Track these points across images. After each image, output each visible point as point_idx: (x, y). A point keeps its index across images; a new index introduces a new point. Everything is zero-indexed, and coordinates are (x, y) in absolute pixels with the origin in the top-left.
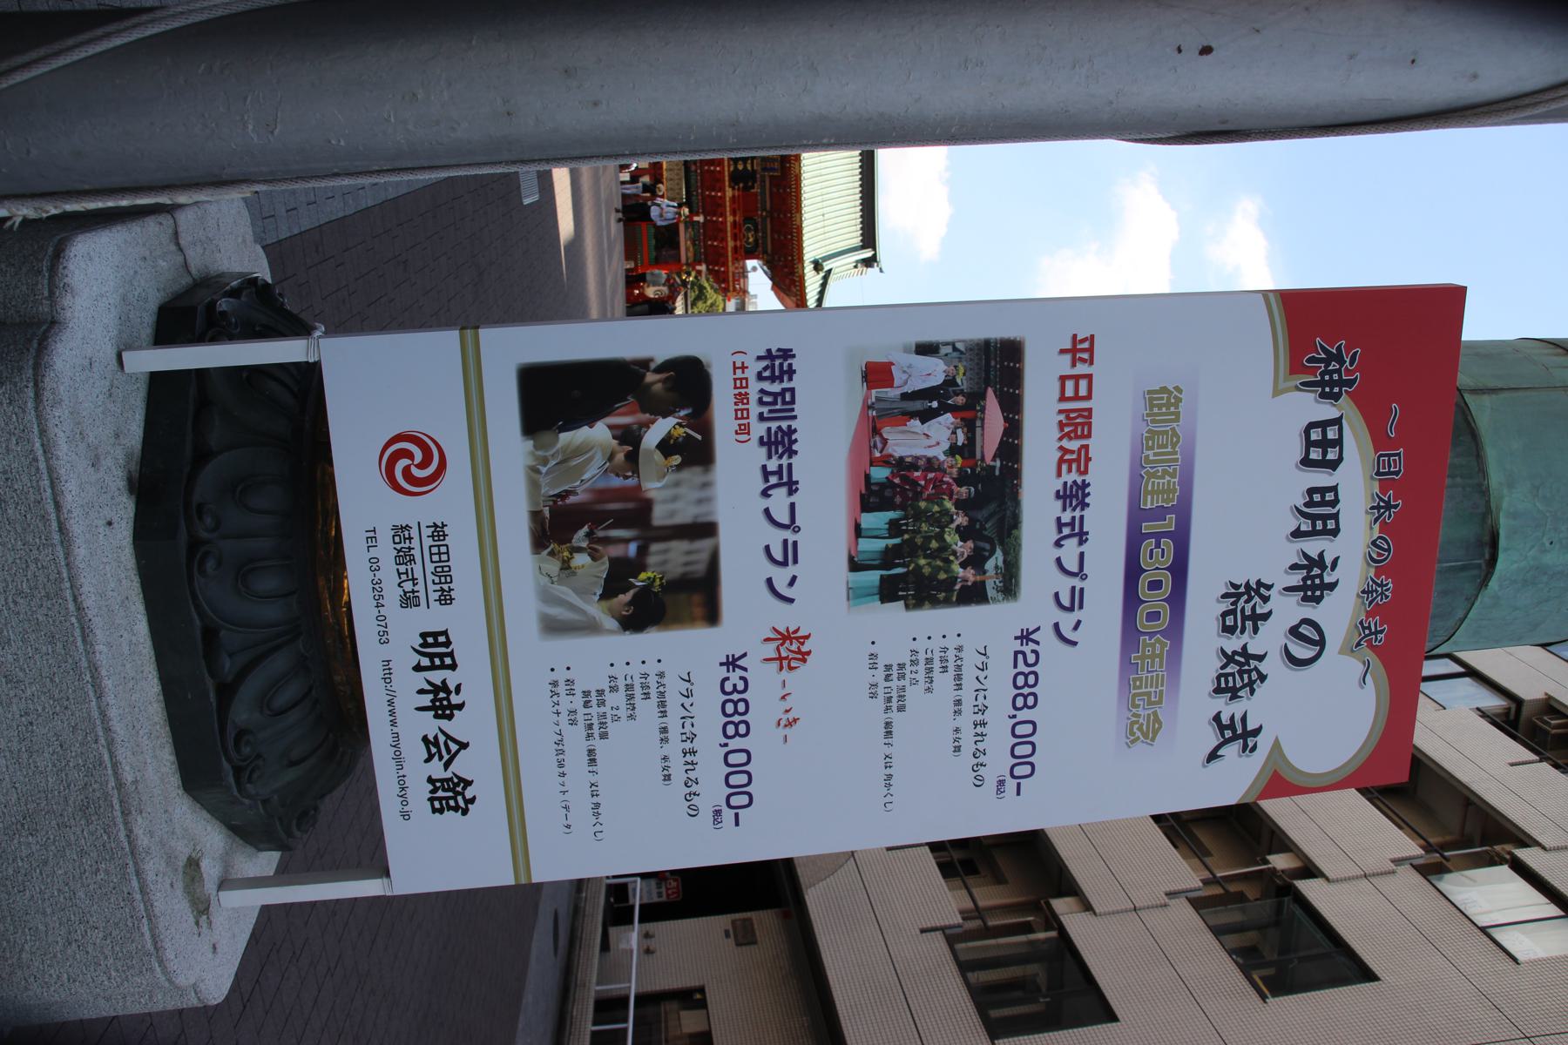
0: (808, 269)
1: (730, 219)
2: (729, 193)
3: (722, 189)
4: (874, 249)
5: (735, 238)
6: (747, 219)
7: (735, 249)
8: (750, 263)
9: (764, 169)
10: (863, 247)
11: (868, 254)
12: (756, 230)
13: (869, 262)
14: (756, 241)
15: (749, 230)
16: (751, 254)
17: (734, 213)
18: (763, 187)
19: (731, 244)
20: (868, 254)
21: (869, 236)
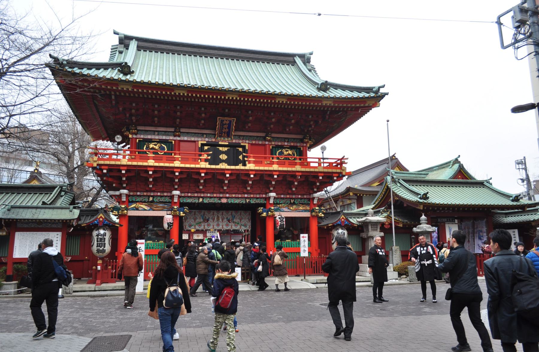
2: (250, 166)
3: (247, 173)
4: (293, 55)
7: (302, 164)
9: (228, 135)
10: (294, 63)
11: (298, 60)
12: (282, 147)
13: (306, 59)
14: (291, 148)
15: (281, 153)
16: (302, 154)
17: (272, 163)
18: (244, 138)
20: (298, 60)
21: (285, 59)
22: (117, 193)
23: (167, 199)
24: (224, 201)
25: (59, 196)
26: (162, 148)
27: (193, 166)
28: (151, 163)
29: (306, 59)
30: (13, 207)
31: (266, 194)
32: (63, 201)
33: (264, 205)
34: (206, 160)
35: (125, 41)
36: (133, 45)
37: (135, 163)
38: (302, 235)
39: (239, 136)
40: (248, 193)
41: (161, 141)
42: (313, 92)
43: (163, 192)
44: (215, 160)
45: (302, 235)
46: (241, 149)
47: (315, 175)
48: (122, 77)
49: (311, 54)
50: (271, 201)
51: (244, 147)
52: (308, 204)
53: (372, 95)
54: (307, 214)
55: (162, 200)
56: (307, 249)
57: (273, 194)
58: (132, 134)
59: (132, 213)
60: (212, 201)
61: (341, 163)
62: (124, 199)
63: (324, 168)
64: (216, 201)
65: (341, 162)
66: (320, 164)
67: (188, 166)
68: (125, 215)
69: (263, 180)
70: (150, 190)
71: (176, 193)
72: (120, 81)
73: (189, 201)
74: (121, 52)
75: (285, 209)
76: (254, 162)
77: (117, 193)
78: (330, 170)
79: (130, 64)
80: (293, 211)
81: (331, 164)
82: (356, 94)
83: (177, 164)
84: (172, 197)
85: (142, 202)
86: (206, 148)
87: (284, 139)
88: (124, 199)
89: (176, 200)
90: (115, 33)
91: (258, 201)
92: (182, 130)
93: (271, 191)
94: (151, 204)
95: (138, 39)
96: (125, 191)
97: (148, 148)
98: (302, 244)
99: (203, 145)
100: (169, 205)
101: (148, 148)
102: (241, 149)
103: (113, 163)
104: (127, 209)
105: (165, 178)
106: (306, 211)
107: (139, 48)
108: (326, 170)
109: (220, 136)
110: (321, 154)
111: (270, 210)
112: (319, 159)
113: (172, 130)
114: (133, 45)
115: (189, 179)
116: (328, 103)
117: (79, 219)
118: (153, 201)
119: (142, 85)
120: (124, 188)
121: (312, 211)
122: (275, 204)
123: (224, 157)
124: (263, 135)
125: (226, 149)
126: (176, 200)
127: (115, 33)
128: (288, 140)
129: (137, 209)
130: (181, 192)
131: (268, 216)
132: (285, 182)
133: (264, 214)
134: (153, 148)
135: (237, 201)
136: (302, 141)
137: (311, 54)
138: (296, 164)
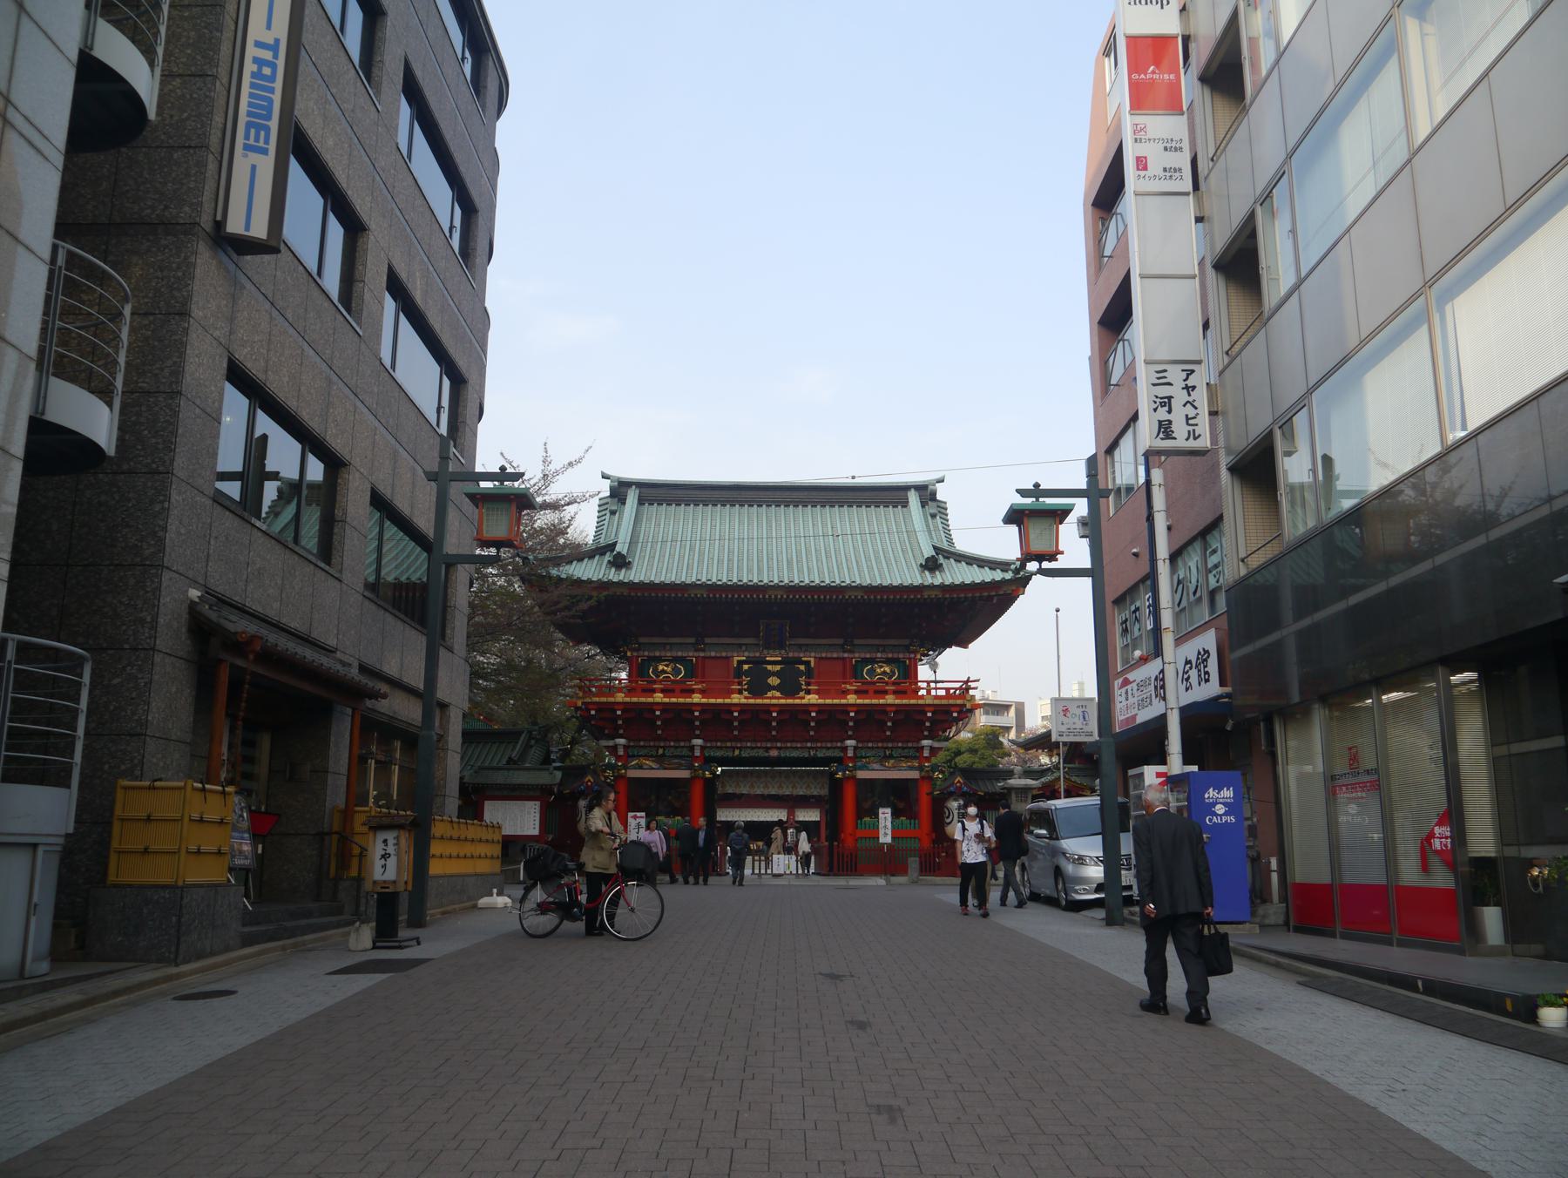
0: (938, 579)
1: (852, 699)
2: (813, 699)
3: (806, 709)
4: (905, 488)
5: (884, 693)
6: (856, 674)
7: (898, 693)
8: (924, 672)
9: (781, 646)
10: (905, 504)
11: (913, 498)
12: (873, 661)
13: (927, 493)
14: (888, 661)
15: (872, 672)
16: (910, 674)
17: (845, 693)
19: (890, 699)
20: (913, 498)
21: (889, 496)
22: (611, 743)
23: (685, 752)
24: (774, 753)
25: (527, 747)
26: (676, 671)
27: (720, 701)
28: (659, 697)
29: (927, 493)
30: (481, 768)
31: (842, 741)
32: (535, 753)
33: (840, 761)
34: (740, 692)
35: (620, 490)
36: (632, 497)
37: (635, 700)
38: (881, 810)
39: (800, 646)
40: (812, 739)
41: (675, 660)
42: (912, 576)
43: (678, 741)
44: (758, 688)
45: (881, 810)
46: (802, 667)
47: (920, 710)
48: (614, 576)
49: (941, 480)
50: (850, 754)
51: (807, 663)
52: (915, 758)
53: (1009, 576)
54: (915, 775)
55: (678, 752)
56: (889, 832)
57: (850, 743)
58: (633, 650)
59: (632, 774)
60: (754, 753)
61: (968, 689)
62: (621, 752)
63: (936, 697)
64: (761, 753)
65: (966, 686)
66: (929, 692)
67: (712, 701)
68: (623, 777)
69: (833, 720)
70: (659, 738)
71: (698, 742)
72: (610, 584)
73: (719, 754)
74: (613, 513)
75: (876, 766)
76: (817, 692)
77: (611, 743)
78: (944, 702)
79: (625, 552)
80: (889, 769)
81: (948, 690)
82: (988, 575)
83: (696, 698)
84: (692, 748)
85: (647, 757)
86: (746, 667)
87: (878, 648)
88: (621, 752)
89: (697, 753)
90: (605, 477)
91: (829, 753)
92: (707, 640)
93: (850, 738)
94: (661, 761)
95: (640, 485)
96: (622, 741)
97: (655, 671)
98: (882, 823)
99: (740, 663)
100: (687, 760)
101: (655, 671)
102: (802, 667)
103: (604, 700)
104: (625, 767)
105: (679, 720)
106: (911, 768)
107: (641, 502)
108: (937, 702)
109: (768, 648)
110: (947, 669)
111: (847, 768)
112: (928, 683)
113: (692, 640)
114: (632, 497)
115: (716, 719)
116: (933, 594)
117: (560, 784)
118: (663, 755)
119: (642, 586)
120: (621, 736)
121: (921, 768)
122: (854, 758)
123: (774, 681)
124: (841, 641)
125: (778, 668)
126: (697, 753)
127: (605, 477)
128: (884, 648)
129: (640, 767)
130: (705, 741)
131: (846, 778)
132: (870, 722)
133: (840, 775)
134: (663, 671)
135: (795, 754)
136: (907, 649)
137: (941, 480)
138: (885, 692)
